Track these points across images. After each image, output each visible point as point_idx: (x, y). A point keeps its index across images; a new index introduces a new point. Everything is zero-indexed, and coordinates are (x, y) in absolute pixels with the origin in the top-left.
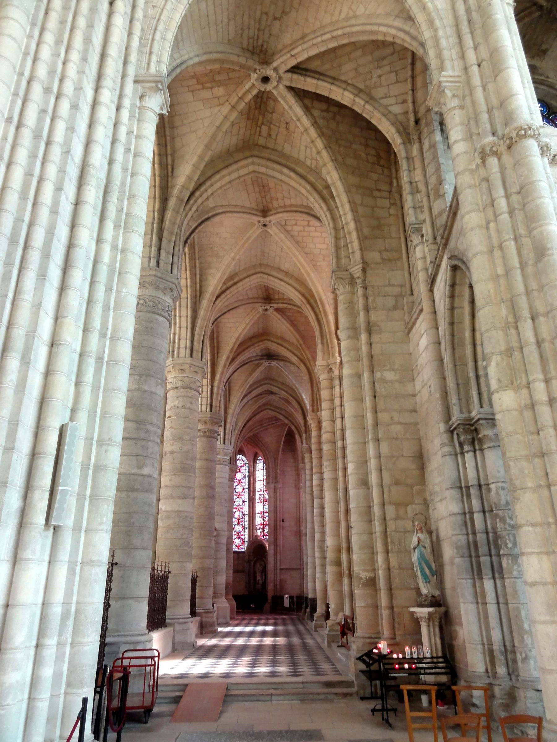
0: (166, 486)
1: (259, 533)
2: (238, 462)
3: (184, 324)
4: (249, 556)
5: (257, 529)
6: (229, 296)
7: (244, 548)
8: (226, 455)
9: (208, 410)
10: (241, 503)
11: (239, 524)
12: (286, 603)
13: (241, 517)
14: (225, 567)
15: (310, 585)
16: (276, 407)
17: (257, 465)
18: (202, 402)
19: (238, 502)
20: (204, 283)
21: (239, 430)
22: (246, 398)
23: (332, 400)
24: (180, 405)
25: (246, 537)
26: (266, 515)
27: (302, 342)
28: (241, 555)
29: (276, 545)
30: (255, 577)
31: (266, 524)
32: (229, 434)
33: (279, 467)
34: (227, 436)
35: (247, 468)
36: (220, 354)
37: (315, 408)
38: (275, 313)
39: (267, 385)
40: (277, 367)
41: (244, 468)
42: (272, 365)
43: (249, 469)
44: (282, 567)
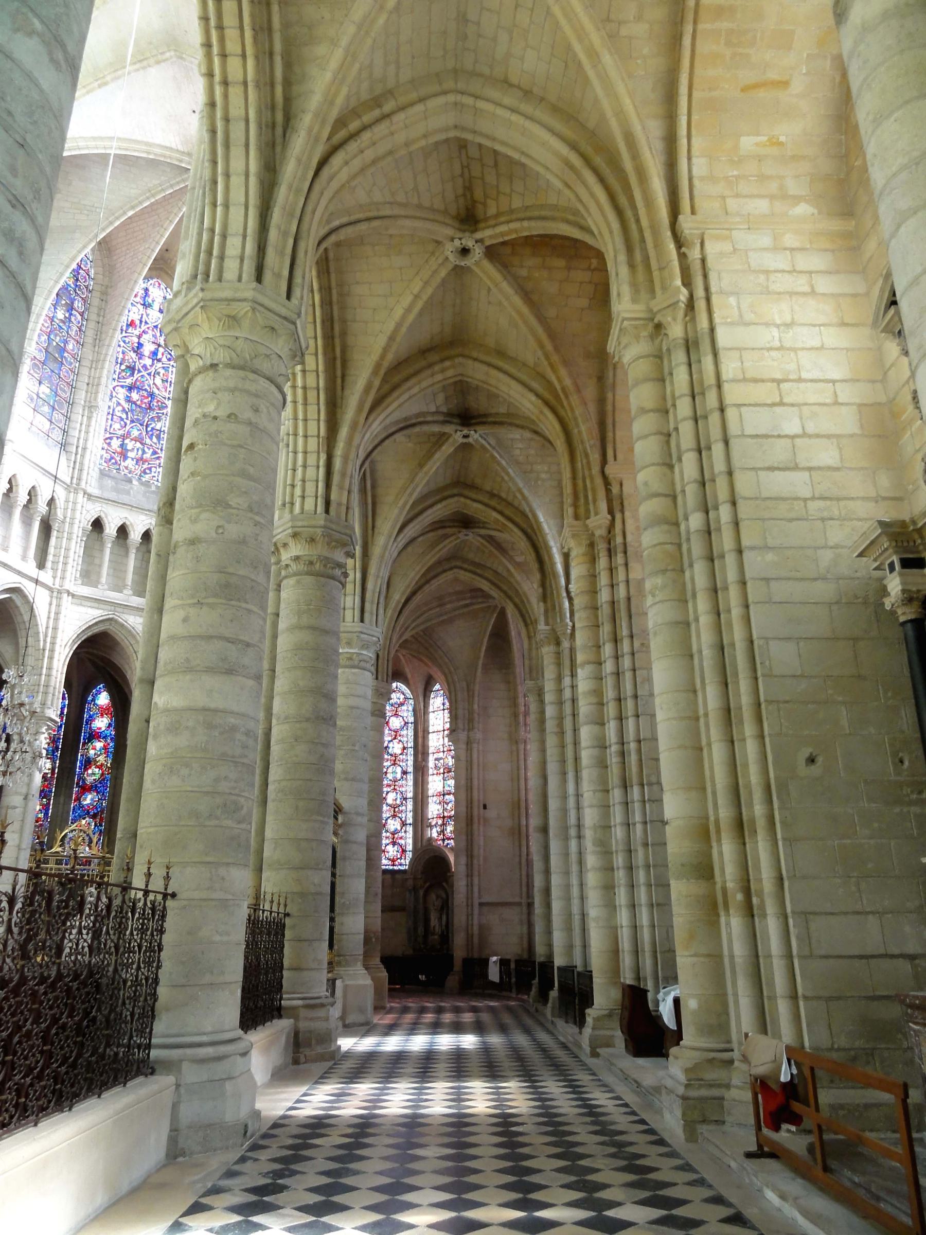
0: (173, 638)
1: (435, 835)
2: (393, 695)
3: (238, 195)
4: (415, 879)
5: (431, 826)
6: (369, 154)
7: (405, 863)
8: (365, 646)
9: (320, 508)
10: (399, 776)
11: (394, 816)
12: (494, 974)
13: (398, 802)
14: (362, 897)
15: (558, 937)
16: (474, 563)
17: (431, 701)
18: (304, 491)
19: (394, 772)
20: (296, 89)
21: (394, 610)
22: (411, 525)
23: (664, 410)
25: (409, 843)
26: (451, 797)
27: (549, 347)
28: (398, 876)
29: (470, 855)
30: (427, 920)
31: (450, 817)
32: (372, 602)
33: (476, 699)
34: (368, 606)
35: (411, 708)
36: (349, 379)
37: (582, 510)
38: (486, 264)
39: (456, 499)
40: (483, 446)
41: (404, 708)
42: (470, 440)
43: (414, 710)
44: (483, 900)
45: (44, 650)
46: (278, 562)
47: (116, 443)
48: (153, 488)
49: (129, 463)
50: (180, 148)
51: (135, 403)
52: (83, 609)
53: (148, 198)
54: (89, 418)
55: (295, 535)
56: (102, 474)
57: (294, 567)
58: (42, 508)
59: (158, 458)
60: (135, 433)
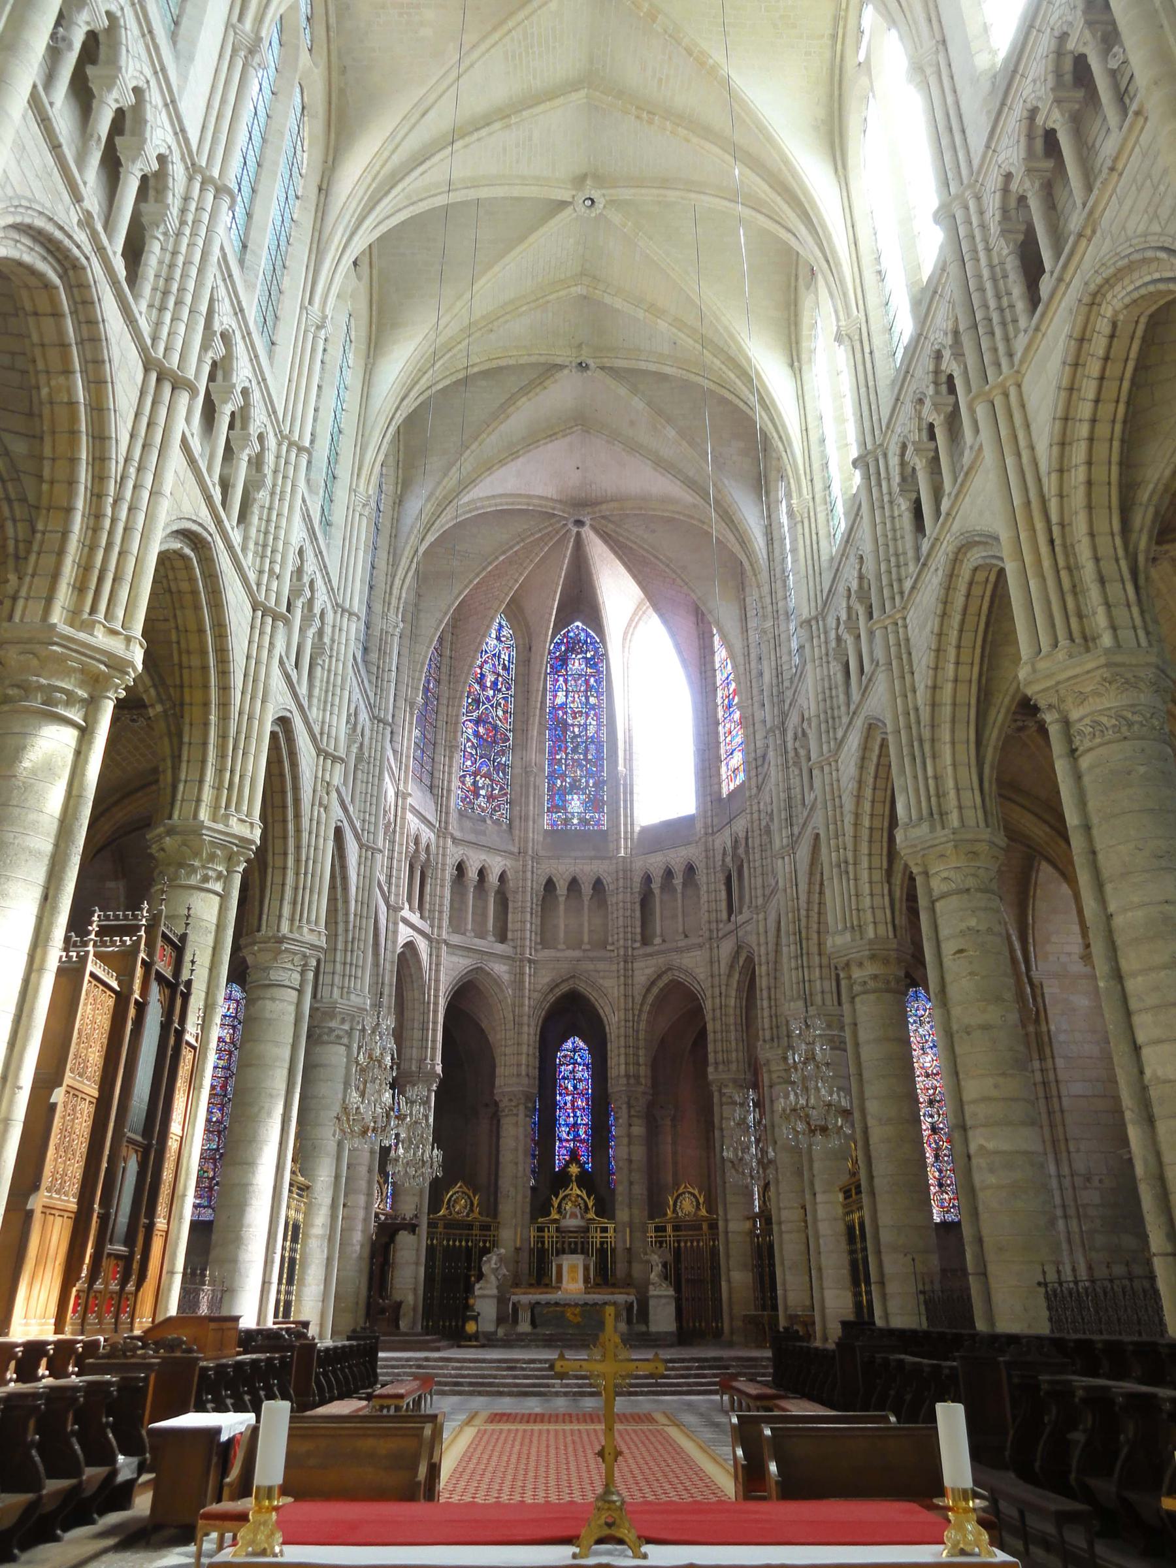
3: (962, 757)
9: (891, 934)
24: (982, 927)
45: (429, 1003)
46: (849, 978)
47: (469, 780)
48: (504, 827)
49: (482, 801)
50: (555, 497)
51: (481, 737)
52: (455, 959)
53: (518, 543)
54: (451, 758)
55: (873, 957)
56: (462, 814)
57: (871, 984)
58: (423, 856)
59: (506, 794)
60: (484, 769)
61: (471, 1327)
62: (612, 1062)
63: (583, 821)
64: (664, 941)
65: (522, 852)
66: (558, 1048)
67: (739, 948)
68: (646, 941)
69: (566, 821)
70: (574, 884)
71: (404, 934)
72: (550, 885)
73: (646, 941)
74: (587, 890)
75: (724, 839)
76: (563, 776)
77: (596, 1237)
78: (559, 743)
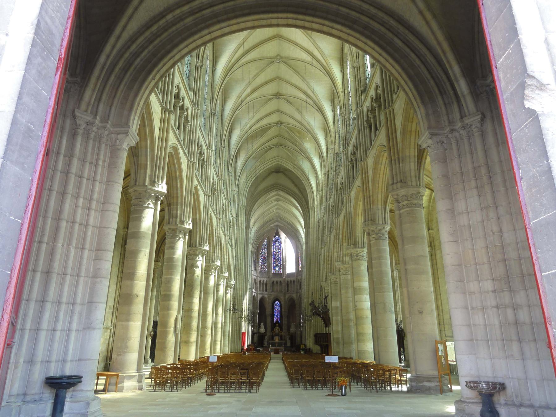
56: (260, 272)
61: (264, 345)
62: (282, 309)
63: (278, 271)
64: (290, 292)
65: (269, 277)
66: (275, 303)
67: (300, 295)
68: (288, 291)
69: (276, 271)
70: (277, 282)
71: (254, 294)
72: (273, 282)
73: (288, 291)
74: (279, 283)
75: (298, 278)
76: (275, 264)
77: (280, 334)
78: (274, 257)
